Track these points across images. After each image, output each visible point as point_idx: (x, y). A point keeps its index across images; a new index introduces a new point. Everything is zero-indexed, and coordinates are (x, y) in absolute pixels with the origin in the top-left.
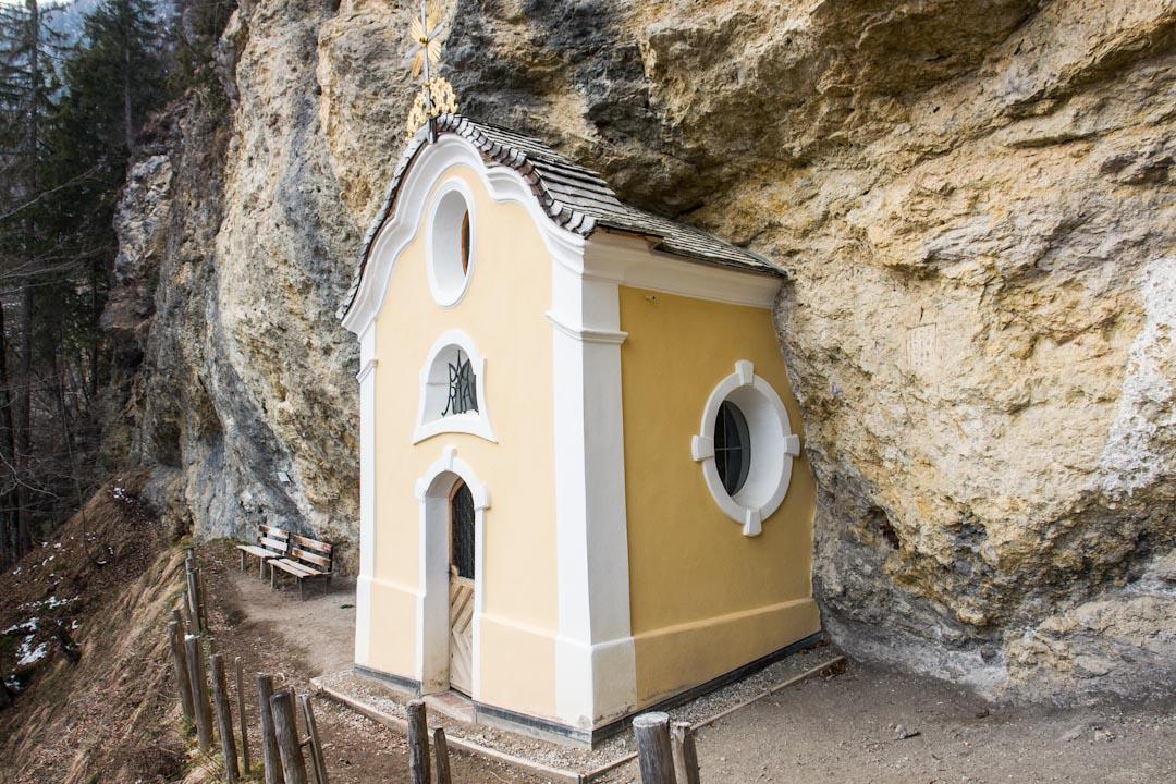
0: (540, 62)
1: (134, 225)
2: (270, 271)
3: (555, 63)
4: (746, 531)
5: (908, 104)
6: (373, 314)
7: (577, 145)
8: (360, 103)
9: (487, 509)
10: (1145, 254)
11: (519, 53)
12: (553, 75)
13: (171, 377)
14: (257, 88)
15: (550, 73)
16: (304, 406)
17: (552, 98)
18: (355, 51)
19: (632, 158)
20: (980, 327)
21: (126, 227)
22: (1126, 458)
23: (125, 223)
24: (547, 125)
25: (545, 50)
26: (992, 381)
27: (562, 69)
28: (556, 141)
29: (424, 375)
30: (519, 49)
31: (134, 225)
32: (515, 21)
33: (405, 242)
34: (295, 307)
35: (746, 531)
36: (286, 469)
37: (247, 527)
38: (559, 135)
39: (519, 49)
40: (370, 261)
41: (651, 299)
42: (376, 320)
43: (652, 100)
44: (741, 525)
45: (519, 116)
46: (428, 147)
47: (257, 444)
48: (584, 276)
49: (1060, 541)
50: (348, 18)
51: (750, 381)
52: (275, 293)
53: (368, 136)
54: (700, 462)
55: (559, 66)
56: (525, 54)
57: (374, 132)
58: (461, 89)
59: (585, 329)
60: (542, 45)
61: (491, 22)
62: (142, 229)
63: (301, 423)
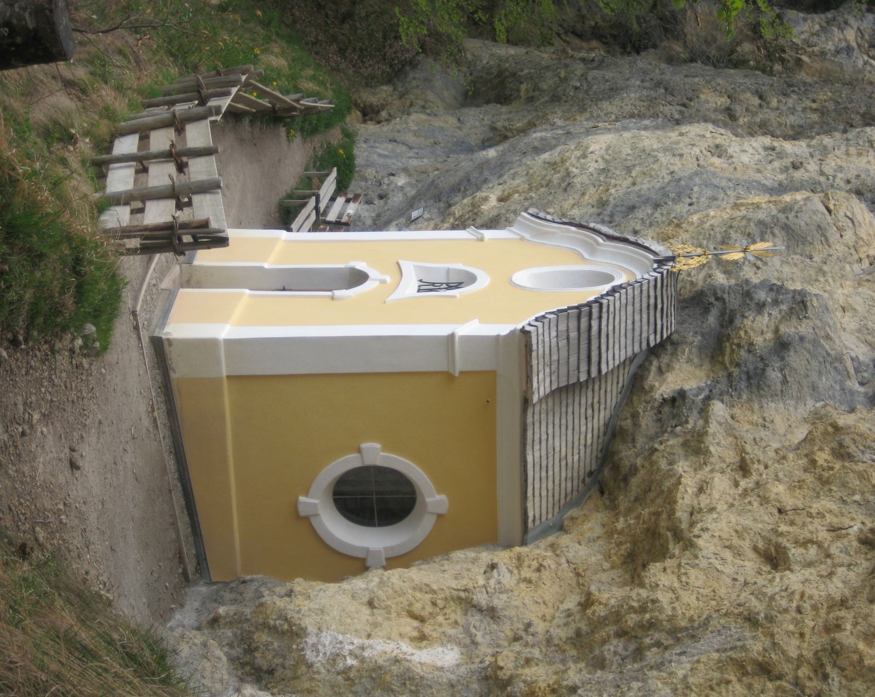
0: (733, 351)
1: (851, 35)
2: (629, 170)
3: (731, 363)
4: (302, 499)
5: (624, 567)
6: (527, 236)
7: (657, 384)
8: (744, 223)
9: (333, 298)
10: (465, 646)
11: (742, 333)
12: (722, 363)
13: (576, 88)
14: (843, 148)
15: (724, 361)
16: (486, 218)
17: (707, 366)
18: (797, 217)
19: (640, 426)
20: (435, 587)
21: (846, 23)
22: (327, 643)
23: (852, 21)
24: (678, 360)
25: (743, 353)
26: (393, 588)
27: (726, 368)
28: (664, 370)
29: (460, 266)
30: (746, 332)
31: (851, 35)
32: (777, 330)
33: (581, 251)
34: (587, 197)
35: (302, 499)
36: (426, 216)
37: (363, 184)
38: (668, 371)
39: (746, 332)
40: (573, 229)
41: (489, 403)
42: (522, 239)
43: (679, 428)
44: (306, 494)
45: (690, 339)
46: (652, 257)
47: (460, 183)
48: (498, 336)
49: (273, 630)
50: (849, 214)
51: (430, 508)
52: (606, 177)
53: (712, 233)
54: (359, 451)
55: (728, 365)
56: (740, 337)
57: (715, 237)
58: (726, 296)
59: (457, 339)
60: (749, 351)
61: (780, 313)
62: (843, 44)
63: (469, 218)
